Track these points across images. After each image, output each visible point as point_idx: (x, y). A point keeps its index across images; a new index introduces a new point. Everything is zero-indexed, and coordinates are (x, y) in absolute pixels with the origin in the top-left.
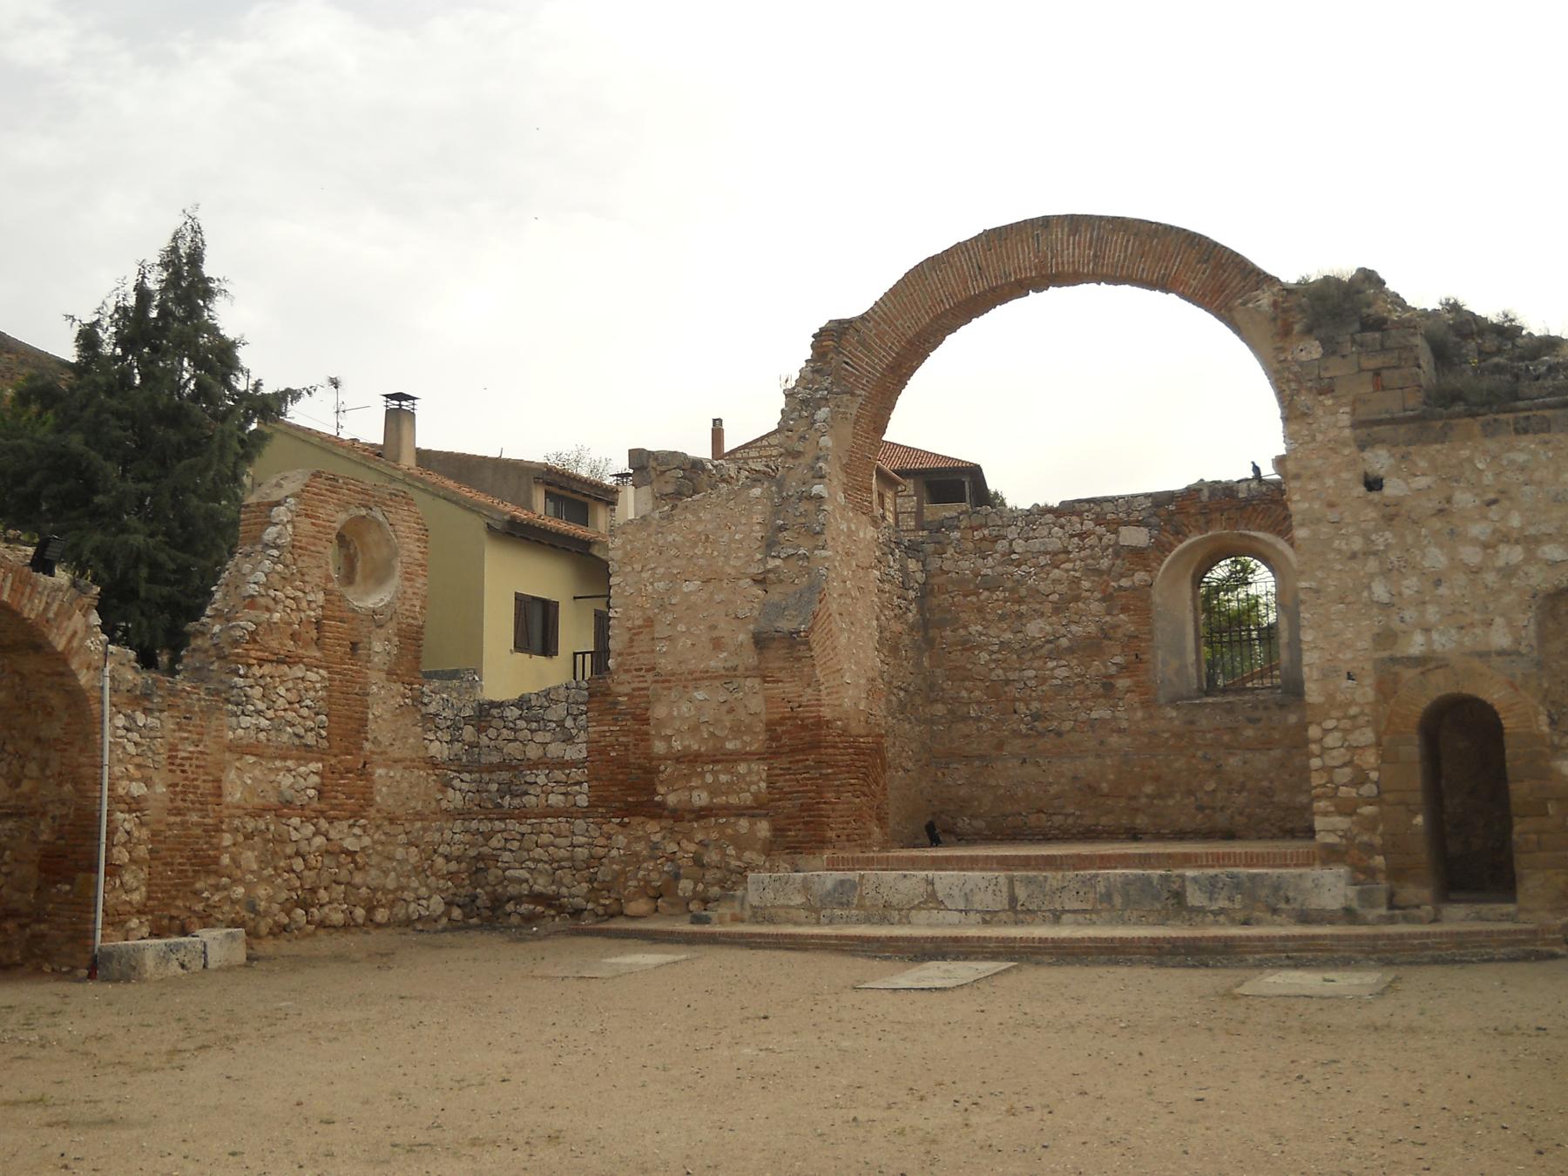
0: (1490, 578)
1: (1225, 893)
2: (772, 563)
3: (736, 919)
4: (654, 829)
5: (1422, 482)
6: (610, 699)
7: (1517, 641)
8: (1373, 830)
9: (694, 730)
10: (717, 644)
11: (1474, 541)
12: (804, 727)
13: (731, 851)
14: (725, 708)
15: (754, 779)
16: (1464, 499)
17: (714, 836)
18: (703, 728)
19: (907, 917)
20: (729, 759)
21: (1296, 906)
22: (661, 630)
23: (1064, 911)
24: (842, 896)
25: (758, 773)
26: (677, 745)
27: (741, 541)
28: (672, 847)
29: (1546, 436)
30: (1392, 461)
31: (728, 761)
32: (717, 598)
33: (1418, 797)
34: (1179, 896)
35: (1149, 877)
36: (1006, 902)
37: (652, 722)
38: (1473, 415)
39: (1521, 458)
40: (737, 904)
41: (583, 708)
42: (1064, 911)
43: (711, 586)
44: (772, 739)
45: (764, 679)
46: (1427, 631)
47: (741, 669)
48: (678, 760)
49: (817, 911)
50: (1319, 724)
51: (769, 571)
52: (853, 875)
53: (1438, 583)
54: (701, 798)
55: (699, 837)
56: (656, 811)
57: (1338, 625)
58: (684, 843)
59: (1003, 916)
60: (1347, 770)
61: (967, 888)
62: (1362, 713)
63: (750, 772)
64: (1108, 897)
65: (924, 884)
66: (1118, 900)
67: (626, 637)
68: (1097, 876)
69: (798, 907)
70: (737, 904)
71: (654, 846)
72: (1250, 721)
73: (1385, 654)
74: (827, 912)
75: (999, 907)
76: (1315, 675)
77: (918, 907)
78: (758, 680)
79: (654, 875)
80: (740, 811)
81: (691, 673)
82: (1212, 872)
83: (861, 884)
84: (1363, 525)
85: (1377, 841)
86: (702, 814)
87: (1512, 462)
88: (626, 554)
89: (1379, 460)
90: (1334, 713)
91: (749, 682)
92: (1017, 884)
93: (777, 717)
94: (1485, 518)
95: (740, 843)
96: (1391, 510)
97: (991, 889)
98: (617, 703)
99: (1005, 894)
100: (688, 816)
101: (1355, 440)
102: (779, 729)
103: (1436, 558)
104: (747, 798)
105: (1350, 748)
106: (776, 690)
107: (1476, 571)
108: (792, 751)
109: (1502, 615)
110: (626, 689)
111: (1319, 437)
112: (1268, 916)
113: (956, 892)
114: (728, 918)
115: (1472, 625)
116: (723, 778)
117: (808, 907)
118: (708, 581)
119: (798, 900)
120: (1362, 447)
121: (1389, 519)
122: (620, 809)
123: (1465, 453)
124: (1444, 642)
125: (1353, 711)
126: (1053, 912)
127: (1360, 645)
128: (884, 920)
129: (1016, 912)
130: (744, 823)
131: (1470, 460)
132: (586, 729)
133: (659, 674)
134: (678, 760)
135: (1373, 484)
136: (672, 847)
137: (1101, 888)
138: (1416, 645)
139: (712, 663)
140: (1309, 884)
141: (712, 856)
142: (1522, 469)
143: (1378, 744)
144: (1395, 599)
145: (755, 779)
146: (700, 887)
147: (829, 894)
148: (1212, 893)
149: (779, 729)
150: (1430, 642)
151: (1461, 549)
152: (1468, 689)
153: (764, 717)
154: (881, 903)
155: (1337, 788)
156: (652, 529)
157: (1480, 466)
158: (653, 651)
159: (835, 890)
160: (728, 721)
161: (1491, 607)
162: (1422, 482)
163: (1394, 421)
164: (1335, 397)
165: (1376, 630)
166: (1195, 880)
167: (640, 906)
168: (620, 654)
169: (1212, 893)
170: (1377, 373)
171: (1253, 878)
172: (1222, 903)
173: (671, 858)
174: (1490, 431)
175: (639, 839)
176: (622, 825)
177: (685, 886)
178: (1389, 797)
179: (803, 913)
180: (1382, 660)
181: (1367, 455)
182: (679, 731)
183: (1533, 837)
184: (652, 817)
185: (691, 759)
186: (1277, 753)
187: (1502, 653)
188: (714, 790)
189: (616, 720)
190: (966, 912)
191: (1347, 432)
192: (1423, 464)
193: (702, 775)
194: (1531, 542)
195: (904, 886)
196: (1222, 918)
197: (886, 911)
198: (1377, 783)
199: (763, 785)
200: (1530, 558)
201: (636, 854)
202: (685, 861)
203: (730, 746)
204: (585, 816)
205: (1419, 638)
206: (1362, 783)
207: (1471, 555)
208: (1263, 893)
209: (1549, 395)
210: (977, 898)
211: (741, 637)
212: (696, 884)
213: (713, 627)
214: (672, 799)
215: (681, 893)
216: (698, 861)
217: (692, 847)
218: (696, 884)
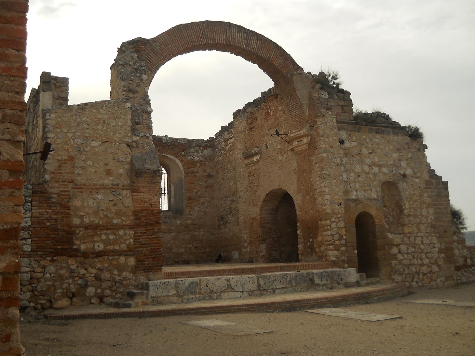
0: (371, 176)
1: (325, 278)
2: (135, 138)
3: (144, 304)
4: (72, 263)
5: (354, 144)
6: (46, 195)
7: (378, 196)
8: (344, 255)
9: (96, 213)
10: (109, 173)
11: (367, 164)
12: (153, 214)
13: (115, 272)
14: (112, 203)
15: (128, 237)
16: (364, 151)
17: (106, 265)
18: (101, 213)
19: (220, 296)
20: (115, 228)
21: (344, 281)
22: (78, 163)
23: (277, 289)
24: (192, 289)
25: (129, 235)
26: (86, 220)
27: (121, 126)
28: (83, 271)
29: (382, 135)
30: (346, 136)
31: (113, 229)
32: (109, 151)
33: (355, 245)
34: (312, 280)
35: (302, 274)
36: (257, 286)
37: (72, 208)
38: (367, 126)
39: (377, 141)
40: (144, 297)
41: (30, 199)
42: (277, 289)
43: (106, 145)
44: (136, 219)
45: (133, 191)
46: (356, 191)
47: (121, 186)
48: (86, 228)
49: (182, 297)
50: (330, 220)
51: (134, 141)
52: (196, 279)
53: (359, 176)
54: (100, 247)
55: (99, 266)
56: (74, 253)
57: (334, 187)
58: (90, 269)
59: (256, 292)
60: (337, 235)
61: (243, 282)
62: (341, 217)
63: (125, 234)
64: (290, 282)
65: (226, 282)
66: (294, 283)
67: (57, 165)
68: (286, 274)
69: (173, 296)
70: (144, 297)
71: (72, 271)
72: (164, 222)
73: (346, 198)
74: (187, 297)
75: (254, 289)
76: (329, 203)
77: (224, 292)
78: (129, 191)
79: (72, 286)
80: (120, 253)
81: (95, 185)
82: (321, 271)
83: (200, 283)
84: (340, 155)
85: (346, 259)
86: (99, 254)
87: (375, 142)
88: (58, 123)
89: (344, 135)
90: (335, 216)
91: (124, 192)
92: (260, 279)
93: (139, 209)
94: (369, 157)
95: (120, 268)
96: (347, 151)
97: (251, 282)
98: (52, 198)
99: (256, 284)
100: (91, 256)
101: (338, 127)
102: (140, 215)
103: (358, 168)
104: (124, 247)
105: (339, 228)
106: (139, 196)
107: (368, 174)
108: (146, 225)
109: (374, 188)
110: (56, 190)
111: (328, 124)
112: (337, 285)
113: (238, 284)
114: (140, 304)
115: (367, 190)
116: (111, 237)
117: (178, 295)
118: (105, 142)
119: (173, 292)
120: (339, 130)
121: (346, 154)
122: (51, 253)
123: (364, 137)
124: (361, 195)
125: (339, 216)
126: (273, 289)
127: (340, 194)
128: (211, 298)
129: (260, 291)
130: (122, 259)
131: (365, 139)
132: (30, 210)
133: (76, 185)
134: (86, 228)
135: (342, 142)
136: (83, 271)
137: (288, 279)
138: (354, 195)
139: (106, 182)
140: (348, 274)
141: (106, 275)
142: (378, 144)
143: (345, 227)
144: (348, 180)
145: (129, 237)
146: (99, 291)
147: (187, 288)
148: (321, 278)
149: (140, 215)
150: (357, 195)
151: (364, 166)
152: (367, 211)
153: (132, 209)
154: (208, 291)
155: (335, 241)
156: (73, 113)
157: (368, 141)
158: (73, 173)
159: (189, 286)
160: (113, 209)
161: (372, 185)
162: (354, 144)
163: (348, 123)
164: (331, 112)
165: (344, 190)
166: (316, 274)
167: (64, 302)
168: (52, 173)
169: (321, 278)
170: (342, 106)
171: (332, 272)
172: (325, 282)
173: (83, 277)
174: (370, 131)
175: (62, 268)
176: (53, 261)
177: (91, 291)
178: (348, 244)
179: (175, 298)
180: (346, 199)
181: (340, 132)
182: (88, 214)
183: (383, 256)
184: (71, 256)
185: (95, 228)
186: (174, 234)
187: (374, 199)
188: (106, 243)
189: (51, 206)
190: (243, 292)
191: (335, 124)
192: (354, 138)
193: (100, 235)
194: (380, 166)
195: (217, 283)
196: (324, 287)
197: (211, 295)
198: (345, 240)
199: (132, 240)
200: (380, 171)
201: (61, 276)
202: (90, 278)
203: (115, 221)
204: (29, 256)
205: (355, 193)
206: (341, 240)
207: (366, 168)
208: (335, 277)
209: (383, 123)
210: (246, 286)
211: (121, 170)
212: (96, 289)
213: (106, 164)
214: (83, 247)
215: (87, 294)
216: (98, 278)
217: (94, 271)
218: (96, 289)
